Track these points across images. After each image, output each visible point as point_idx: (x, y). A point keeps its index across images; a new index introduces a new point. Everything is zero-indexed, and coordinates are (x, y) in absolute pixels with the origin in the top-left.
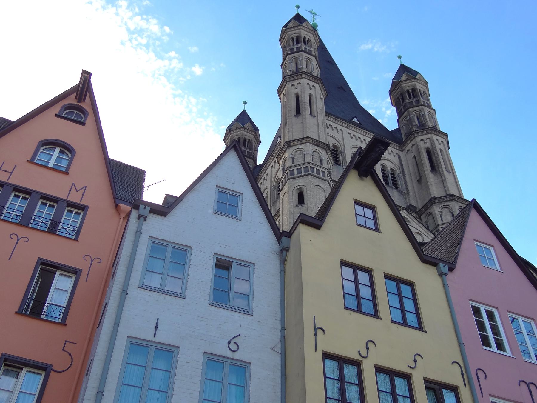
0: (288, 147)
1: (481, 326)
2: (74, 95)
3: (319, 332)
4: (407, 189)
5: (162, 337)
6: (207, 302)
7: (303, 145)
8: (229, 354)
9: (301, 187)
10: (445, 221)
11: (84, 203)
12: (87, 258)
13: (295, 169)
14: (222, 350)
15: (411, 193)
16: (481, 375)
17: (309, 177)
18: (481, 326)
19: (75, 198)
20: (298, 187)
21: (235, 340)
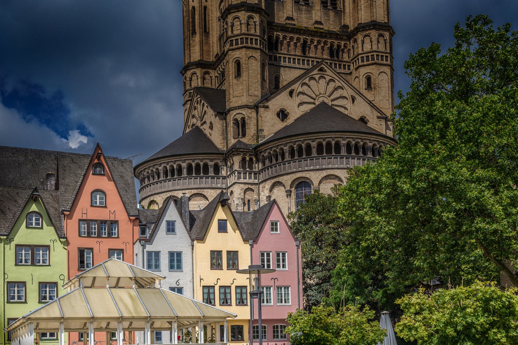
0: (228, 13)
3: (202, 280)
4: (344, 6)
7: (240, 13)
8: (177, 286)
9: (238, 59)
10: (365, 50)
12: (124, 243)
13: (234, 39)
14: (174, 285)
15: (347, 10)
17: (244, 50)
20: (236, 59)
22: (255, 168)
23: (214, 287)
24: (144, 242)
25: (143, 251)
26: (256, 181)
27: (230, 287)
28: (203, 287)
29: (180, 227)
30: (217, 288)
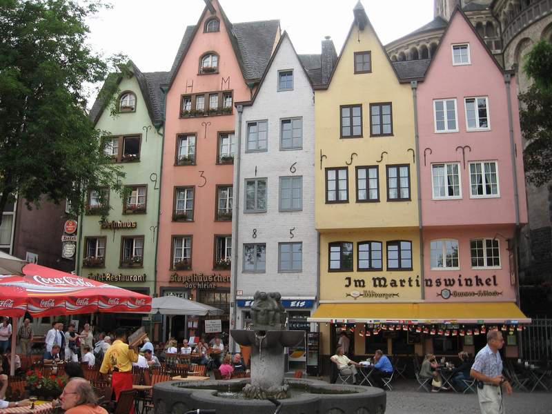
1: (440, 115)
2: (209, 11)
3: (324, 158)
5: (259, 175)
6: (278, 150)
8: (291, 174)
11: (231, 88)
16: (428, 152)
18: (440, 115)
19: (225, 88)
21: (295, 166)
22: (497, 34)
23: (346, 168)
24: (241, 106)
25: (240, 122)
26: (499, 51)
27: (377, 167)
28: (327, 169)
29: (300, 80)
30: (352, 170)
